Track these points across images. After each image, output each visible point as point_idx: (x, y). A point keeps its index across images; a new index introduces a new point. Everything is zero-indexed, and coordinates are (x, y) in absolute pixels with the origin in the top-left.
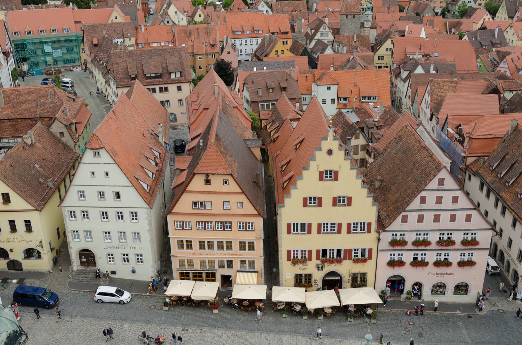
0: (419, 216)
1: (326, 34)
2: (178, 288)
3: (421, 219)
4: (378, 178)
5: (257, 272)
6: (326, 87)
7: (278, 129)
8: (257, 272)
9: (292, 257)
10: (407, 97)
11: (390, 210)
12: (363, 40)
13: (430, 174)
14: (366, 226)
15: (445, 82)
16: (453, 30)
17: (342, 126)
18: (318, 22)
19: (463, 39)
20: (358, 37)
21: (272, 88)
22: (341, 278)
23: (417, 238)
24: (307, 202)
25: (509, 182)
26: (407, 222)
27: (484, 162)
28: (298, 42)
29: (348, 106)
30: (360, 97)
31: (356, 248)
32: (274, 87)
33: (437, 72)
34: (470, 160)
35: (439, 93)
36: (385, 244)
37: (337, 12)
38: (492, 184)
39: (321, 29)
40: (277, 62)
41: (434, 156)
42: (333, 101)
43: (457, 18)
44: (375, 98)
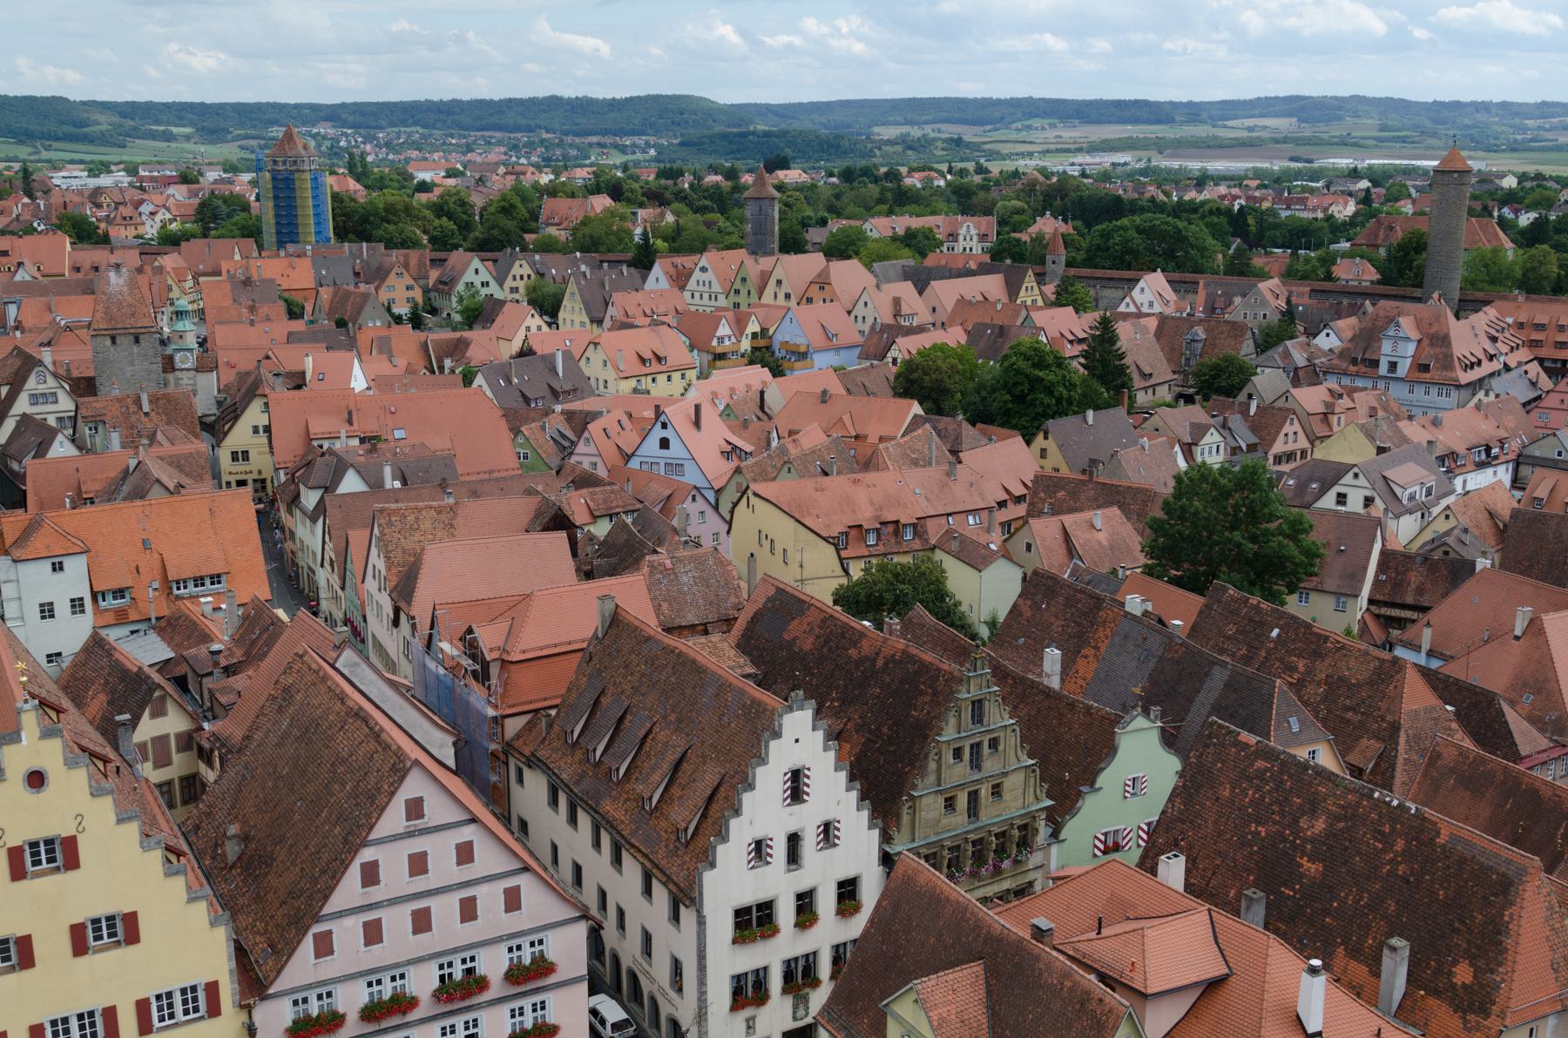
4: (233, 830)
6: (47, 565)
10: (327, 564)
12: (173, 409)
13: (378, 790)
14: (201, 995)
15: (420, 510)
16: (448, 363)
17: (107, 682)
18: (18, 362)
19: (475, 385)
20: (154, 400)
23: (371, 994)
27: (550, 726)
29: (133, 616)
30: (168, 585)
33: (404, 482)
34: (513, 726)
35: (408, 544)
37: (78, 328)
38: (577, 783)
39: (31, 383)
41: (384, 736)
42: (77, 605)
43: (454, 329)
44: (216, 579)
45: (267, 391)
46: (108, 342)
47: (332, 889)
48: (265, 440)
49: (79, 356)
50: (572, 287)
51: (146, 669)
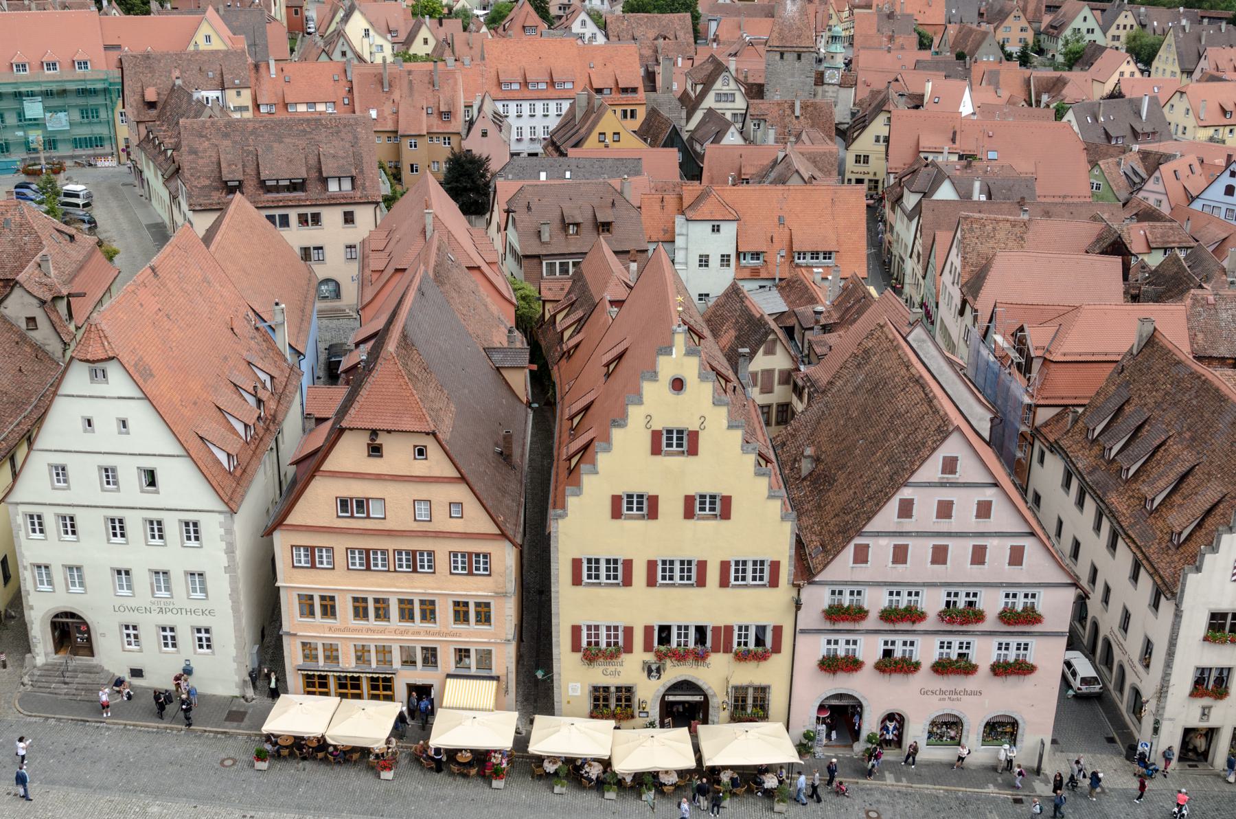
0: (896, 547)
1: (730, 97)
2: (297, 715)
3: (900, 555)
4: (809, 451)
5: (497, 678)
6: (708, 226)
7: (580, 323)
8: (497, 678)
9: (584, 644)
10: (915, 256)
11: (829, 531)
12: (816, 114)
13: (924, 444)
15: (997, 221)
16: (1045, 98)
17: (737, 322)
18: (711, 67)
19: (1065, 120)
20: (804, 107)
21: (577, 225)
22: (706, 697)
24: (619, 506)
25: (1128, 470)
26: (866, 562)
27: (1075, 421)
28: (659, 114)
29: (763, 274)
30: (792, 254)
31: (744, 623)
32: (580, 220)
33: (989, 197)
34: (1043, 415)
35: (984, 248)
36: (811, 615)
38: (1090, 473)
39: (718, 85)
40: (599, 160)
41: (935, 402)
42: (725, 260)
43: (1056, 69)
44: (828, 255)
45: (892, 108)
46: (778, 57)
47: (875, 513)
48: (883, 149)
49: (755, 66)
50: (1170, 39)
51: (766, 317)
